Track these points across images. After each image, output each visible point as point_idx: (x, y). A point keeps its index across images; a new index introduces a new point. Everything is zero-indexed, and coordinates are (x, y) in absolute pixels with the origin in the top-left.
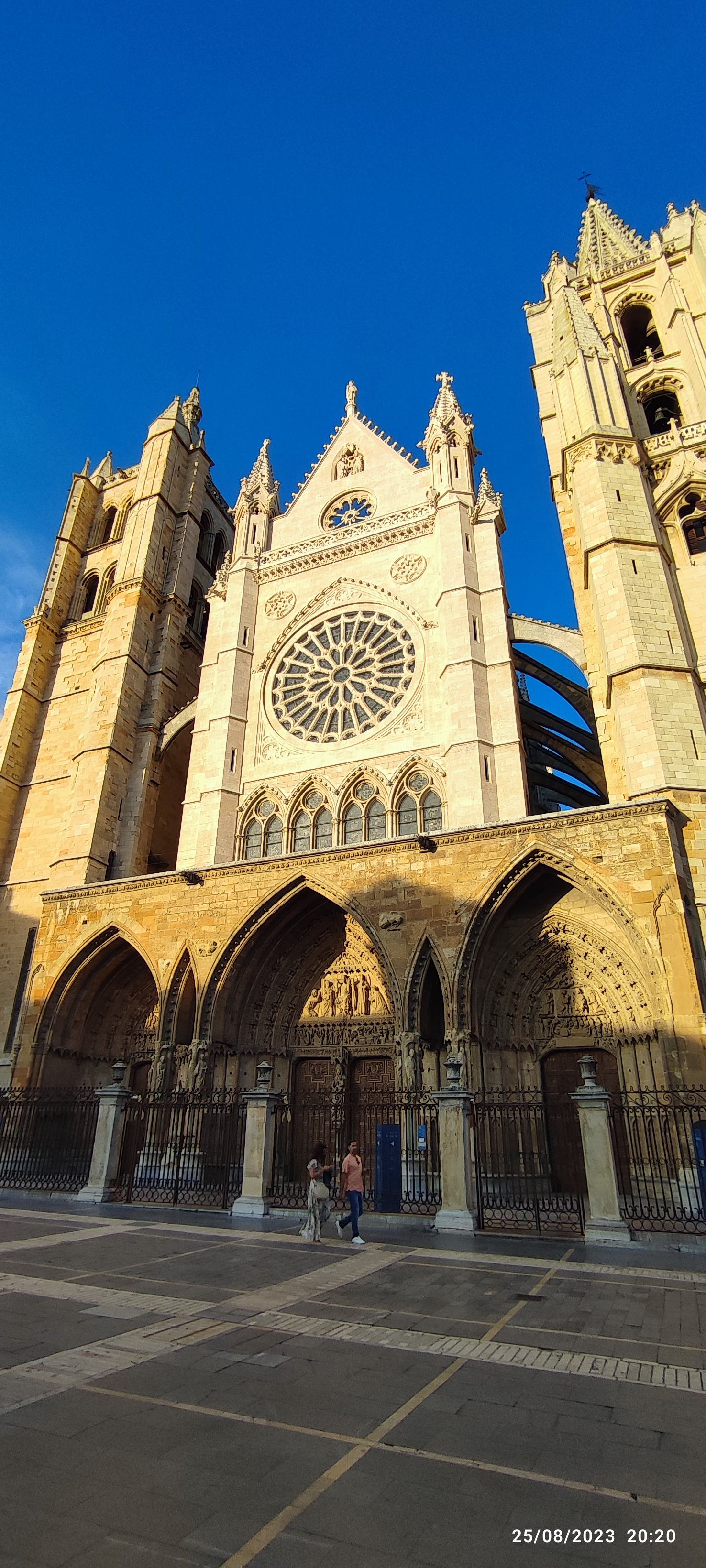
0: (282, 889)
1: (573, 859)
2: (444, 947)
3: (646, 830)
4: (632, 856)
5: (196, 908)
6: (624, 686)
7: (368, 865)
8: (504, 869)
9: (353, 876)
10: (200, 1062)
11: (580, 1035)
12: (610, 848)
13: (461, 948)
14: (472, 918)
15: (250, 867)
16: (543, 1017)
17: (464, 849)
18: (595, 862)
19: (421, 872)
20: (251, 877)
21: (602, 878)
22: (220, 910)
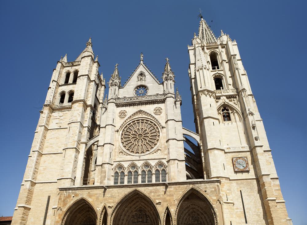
6: (211, 152)
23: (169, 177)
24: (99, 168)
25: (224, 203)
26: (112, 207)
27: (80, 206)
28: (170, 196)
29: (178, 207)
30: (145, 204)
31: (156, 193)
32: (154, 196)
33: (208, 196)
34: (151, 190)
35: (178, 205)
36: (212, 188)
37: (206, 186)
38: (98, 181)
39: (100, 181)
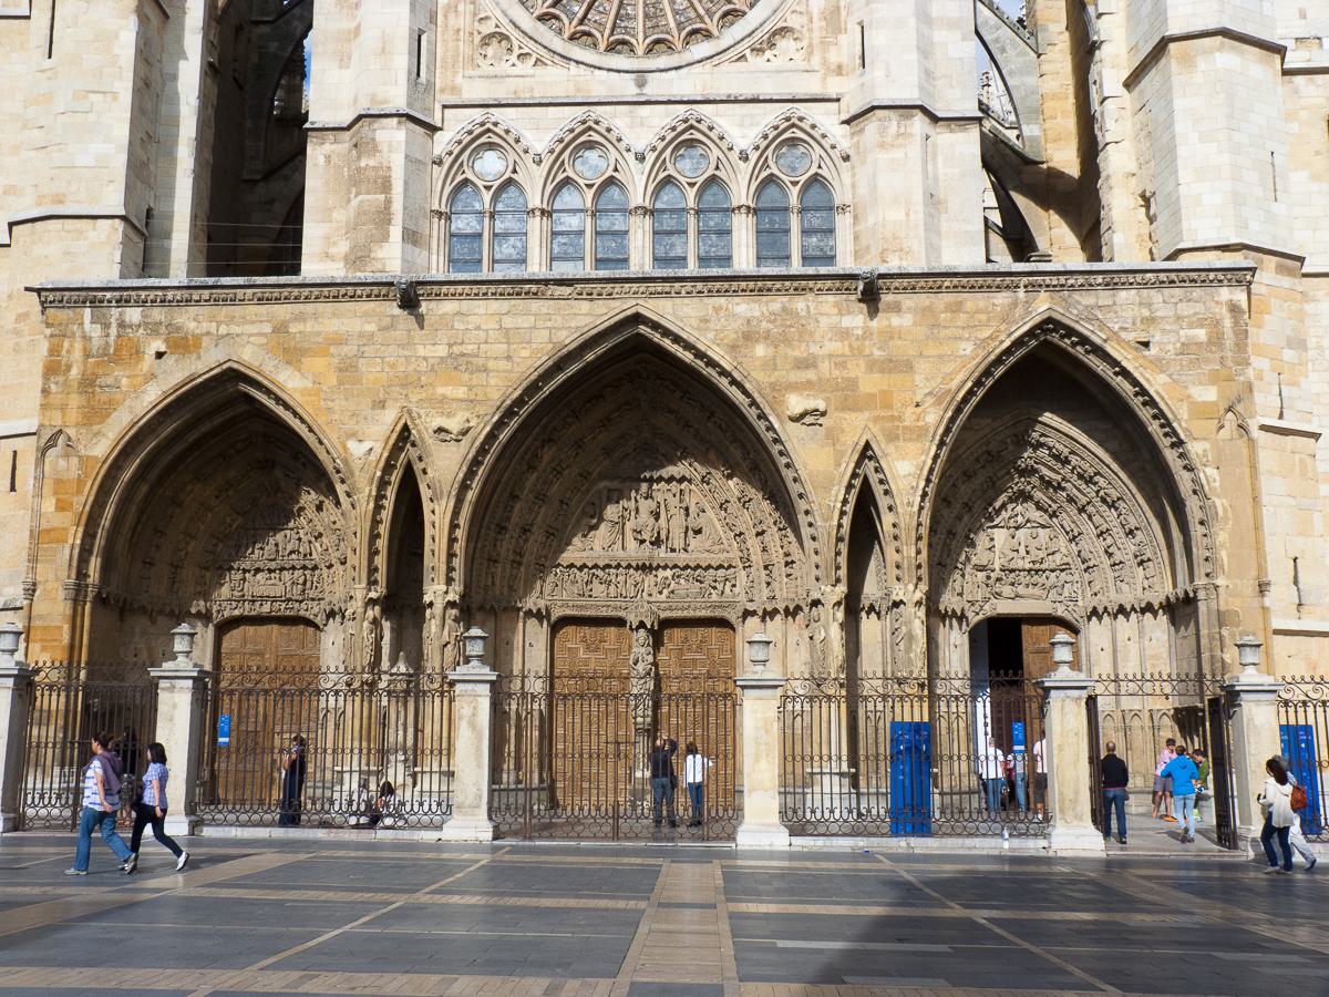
0: (599, 333)
1: (1105, 341)
3: (1217, 310)
5: (421, 351)
6: (1188, 61)
7: (764, 309)
9: (737, 324)
10: (449, 622)
11: (1031, 597)
13: (924, 462)
15: (534, 288)
16: (981, 568)
17: (932, 303)
18: (1137, 348)
20: (535, 305)
21: (1147, 376)
22: (474, 360)
23: (864, 242)
24: (327, 147)
25: (1264, 428)
26: (465, 432)
27: (206, 427)
29: (942, 444)
30: (687, 425)
31: (787, 341)
32: (771, 364)
33: (1163, 378)
34: (748, 321)
35: (947, 430)
36: (1191, 326)
37: (1149, 305)
38: (333, 250)
39: (343, 247)
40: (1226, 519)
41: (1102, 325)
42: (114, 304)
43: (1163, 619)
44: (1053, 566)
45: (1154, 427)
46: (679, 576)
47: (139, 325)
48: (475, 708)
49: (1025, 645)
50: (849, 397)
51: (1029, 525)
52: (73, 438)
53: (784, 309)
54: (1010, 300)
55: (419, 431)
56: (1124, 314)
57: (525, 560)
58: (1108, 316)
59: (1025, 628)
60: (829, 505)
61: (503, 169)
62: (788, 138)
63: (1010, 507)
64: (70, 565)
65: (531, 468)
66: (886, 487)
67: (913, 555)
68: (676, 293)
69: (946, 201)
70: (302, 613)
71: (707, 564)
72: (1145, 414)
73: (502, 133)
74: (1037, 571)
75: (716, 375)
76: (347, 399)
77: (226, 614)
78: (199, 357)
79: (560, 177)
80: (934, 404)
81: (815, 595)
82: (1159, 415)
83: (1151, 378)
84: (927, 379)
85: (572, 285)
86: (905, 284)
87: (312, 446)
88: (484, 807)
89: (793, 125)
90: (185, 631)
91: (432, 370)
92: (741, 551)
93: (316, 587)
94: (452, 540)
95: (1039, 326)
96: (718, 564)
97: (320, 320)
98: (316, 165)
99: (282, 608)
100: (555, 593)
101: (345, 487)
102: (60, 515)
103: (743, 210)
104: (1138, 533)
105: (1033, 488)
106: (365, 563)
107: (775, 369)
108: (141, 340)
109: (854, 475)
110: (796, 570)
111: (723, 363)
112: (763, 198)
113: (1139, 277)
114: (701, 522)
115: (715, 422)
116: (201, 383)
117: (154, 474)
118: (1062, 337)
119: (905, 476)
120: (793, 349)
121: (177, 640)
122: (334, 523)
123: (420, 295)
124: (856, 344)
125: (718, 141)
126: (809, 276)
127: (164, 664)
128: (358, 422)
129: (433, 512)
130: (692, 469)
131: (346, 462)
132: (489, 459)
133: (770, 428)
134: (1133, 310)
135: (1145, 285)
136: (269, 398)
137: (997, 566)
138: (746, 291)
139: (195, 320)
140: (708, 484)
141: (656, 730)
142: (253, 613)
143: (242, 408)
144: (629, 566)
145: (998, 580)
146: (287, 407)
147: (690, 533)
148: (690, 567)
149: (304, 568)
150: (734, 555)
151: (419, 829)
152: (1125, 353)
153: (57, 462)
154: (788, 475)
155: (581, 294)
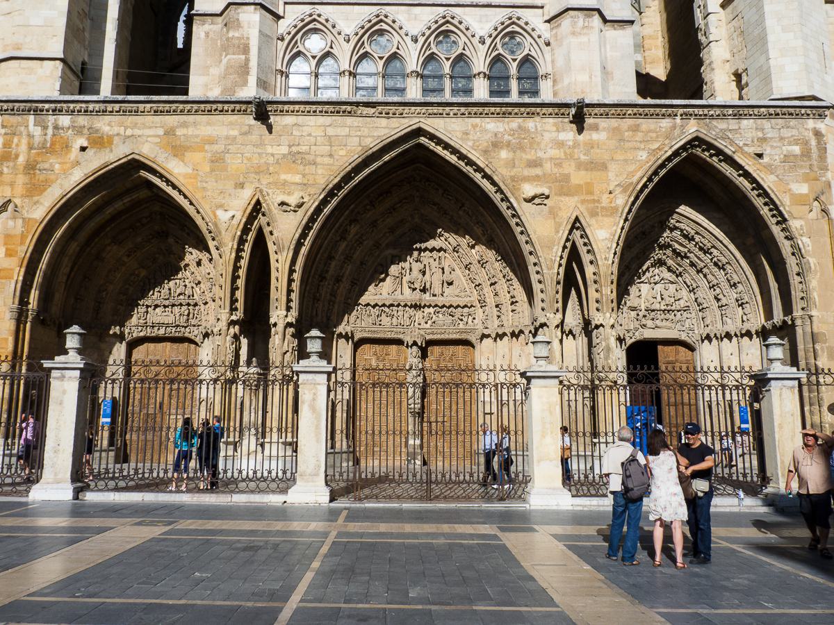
0: (393, 140)
1: (734, 153)
2: (598, 229)
3: (806, 134)
4: (792, 158)
5: (269, 150)
8: (663, 152)
9: (488, 136)
10: (288, 336)
12: (772, 147)
13: (616, 231)
14: (627, 201)
15: (349, 108)
16: (633, 309)
17: (619, 125)
18: (754, 158)
19: (571, 143)
21: (763, 176)
24: (207, 27)
26: (300, 206)
27: (119, 205)
28: (592, 170)
29: (626, 220)
30: (445, 213)
31: (521, 148)
32: (512, 164)
33: (772, 178)
34: (496, 135)
36: (790, 143)
37: (763, 130)
40: (816, 271)
41: (732, 142)
42: (51, 112)
43: (756, 340)
44: (678, 308)
45: (765, 211)
46: (438, 312)
47: (69, 128)
48: (315, 394)
49: (660, 358)
50: (565, 187)
51: (662, 282)
52: (19, 205)
53: (520, 127)
54: (671, 124)
55: (268, 205)
56: (746, 135)
57: (337, 300)
58: (736, 136)
59: (660, 348)
60: (552, 259)
61: (324, 47)
62: (510, 33)
63: (651, 269)
64: (14, 294)
65: (343, 238)
66: (589, 248)
67: (609, 293)
68: (447, 114)
69: (612, 73)
70: (187, 335)
71: (457, 304)
72: (759, 202)
73: (324, 22)
74: (668, 311)
75: (473, 172)
76: (216, 182)
77: (135, 335)
78: (111, 151)
79: (361, 52)
80: (621, 193)
81: (542, 320)
82: (771, 203)
83: (765, 178)
84: (617, 176)
85: (375, 107)
86: (602, 111)
87: (192, 215)
88: (323, 475)
89: (514, 23)
90: (74, 331)
91: (277, 163)
92: (480, 296)
93: (197, 318)
94: (290, 281)
95: (689, 142)
96: (464, 304)
97: (198, 127)
98: (199, 38)
99: (173, 331)
100: (357, 323)
101: (215, 243)
102: (9, 259)
103: (482, 75)
104: (739, 285)
105: (667, 257)
106: (228, 295)
107: (514, 167)
108: (70, 138)
109: (568, 240)
110: (518, 307)
111: (479, 162)
112: (494, 70)
113: (756, 111)
114: (453, 277)
115: (465, 210)
116: (113, 168)
117: (83, 236)
118: (703, 150)
119: (603, 240)
120: (526, 154)
121: (69, 338)
122: (209, 274)
123: (269, 111)
124: (568, 151)
125: (465, 31)
126: (538, 104)
127: (56, 358)
128: (224, 197)
129: (277, 261)
130: (447, 243)
131: (216, 225)
132: (317, 226)
133: (511, 207)
134: (752, 133)
135: (760, 116)
136: (162, 181)
137: (643, 308)
138: (494, 114)
139: (109, 125)
140: (457, 252)
141: (423, 412)
142: (153, 335)
143: (144, 193)
144: (406, 306)
145: (645, 316)
146: (174, 187)
147: (445, 284)
148: (446, 307)
149: (188, 305)
150: (474, 298)
151: (267, 493)
152: (747, 161)
153: (7, 223)
154: (522, 239)
155: (381, 113)
